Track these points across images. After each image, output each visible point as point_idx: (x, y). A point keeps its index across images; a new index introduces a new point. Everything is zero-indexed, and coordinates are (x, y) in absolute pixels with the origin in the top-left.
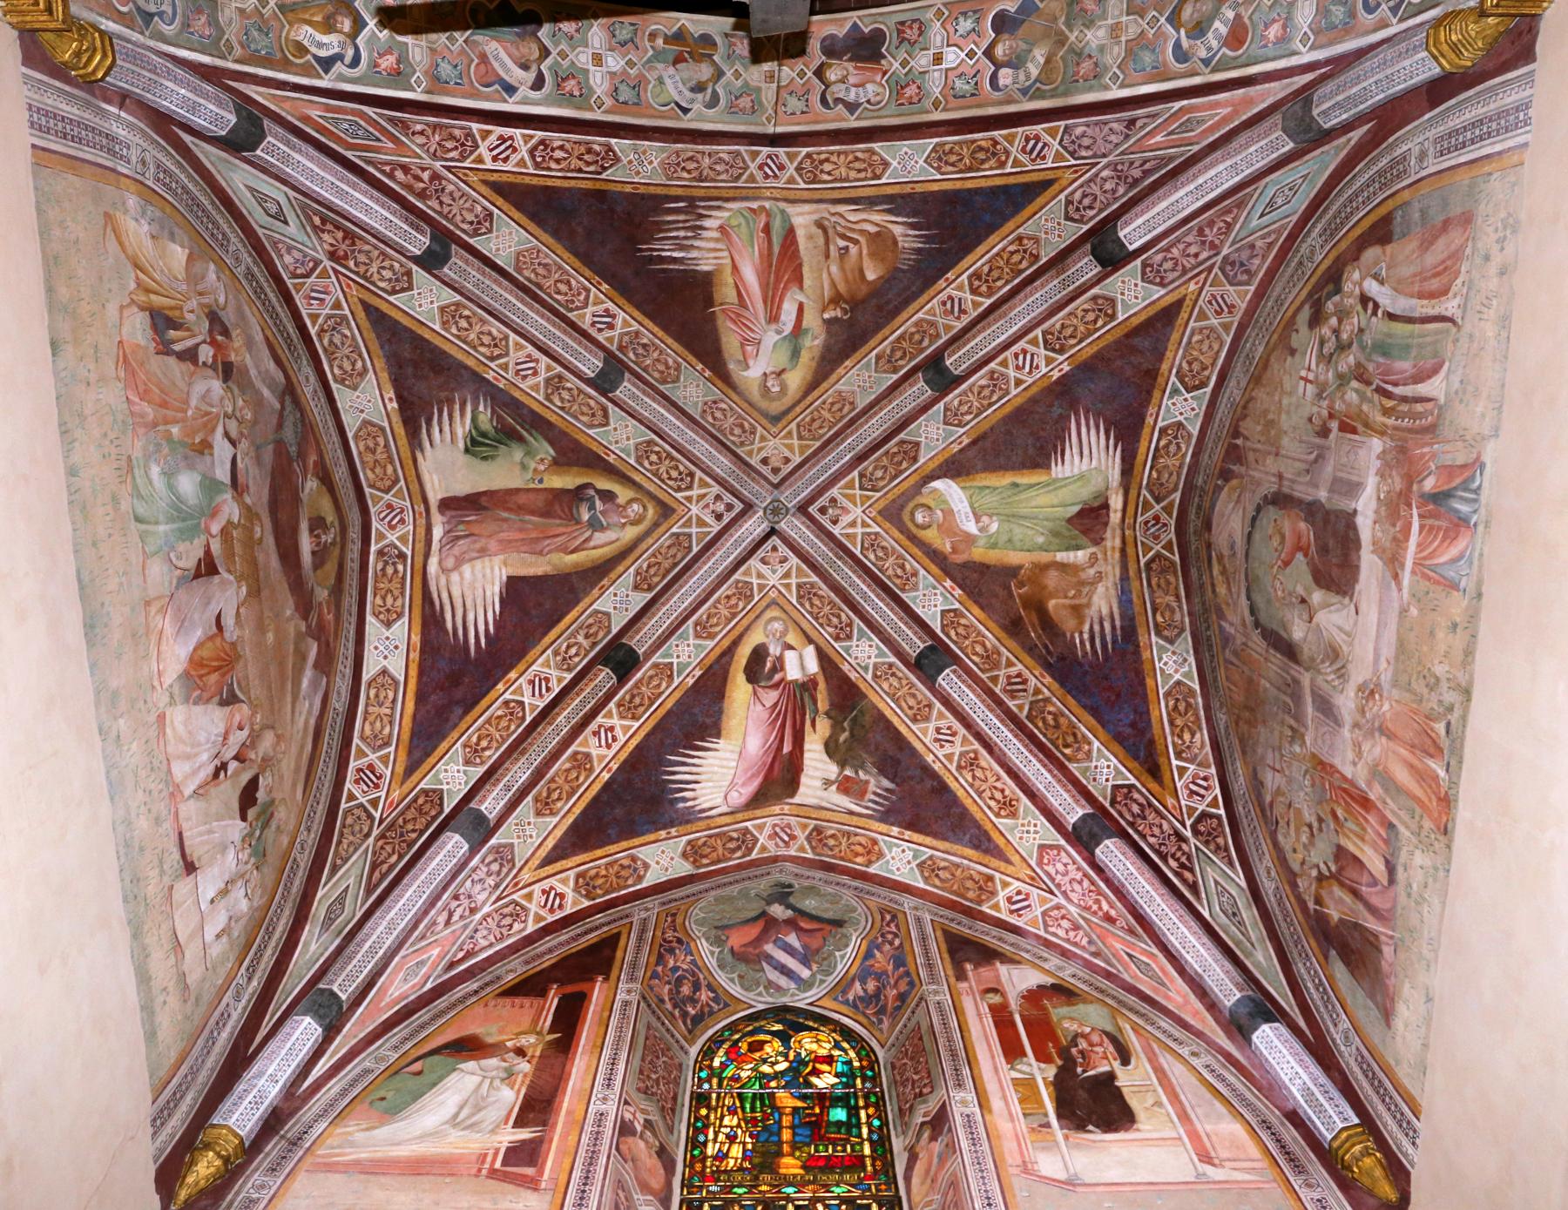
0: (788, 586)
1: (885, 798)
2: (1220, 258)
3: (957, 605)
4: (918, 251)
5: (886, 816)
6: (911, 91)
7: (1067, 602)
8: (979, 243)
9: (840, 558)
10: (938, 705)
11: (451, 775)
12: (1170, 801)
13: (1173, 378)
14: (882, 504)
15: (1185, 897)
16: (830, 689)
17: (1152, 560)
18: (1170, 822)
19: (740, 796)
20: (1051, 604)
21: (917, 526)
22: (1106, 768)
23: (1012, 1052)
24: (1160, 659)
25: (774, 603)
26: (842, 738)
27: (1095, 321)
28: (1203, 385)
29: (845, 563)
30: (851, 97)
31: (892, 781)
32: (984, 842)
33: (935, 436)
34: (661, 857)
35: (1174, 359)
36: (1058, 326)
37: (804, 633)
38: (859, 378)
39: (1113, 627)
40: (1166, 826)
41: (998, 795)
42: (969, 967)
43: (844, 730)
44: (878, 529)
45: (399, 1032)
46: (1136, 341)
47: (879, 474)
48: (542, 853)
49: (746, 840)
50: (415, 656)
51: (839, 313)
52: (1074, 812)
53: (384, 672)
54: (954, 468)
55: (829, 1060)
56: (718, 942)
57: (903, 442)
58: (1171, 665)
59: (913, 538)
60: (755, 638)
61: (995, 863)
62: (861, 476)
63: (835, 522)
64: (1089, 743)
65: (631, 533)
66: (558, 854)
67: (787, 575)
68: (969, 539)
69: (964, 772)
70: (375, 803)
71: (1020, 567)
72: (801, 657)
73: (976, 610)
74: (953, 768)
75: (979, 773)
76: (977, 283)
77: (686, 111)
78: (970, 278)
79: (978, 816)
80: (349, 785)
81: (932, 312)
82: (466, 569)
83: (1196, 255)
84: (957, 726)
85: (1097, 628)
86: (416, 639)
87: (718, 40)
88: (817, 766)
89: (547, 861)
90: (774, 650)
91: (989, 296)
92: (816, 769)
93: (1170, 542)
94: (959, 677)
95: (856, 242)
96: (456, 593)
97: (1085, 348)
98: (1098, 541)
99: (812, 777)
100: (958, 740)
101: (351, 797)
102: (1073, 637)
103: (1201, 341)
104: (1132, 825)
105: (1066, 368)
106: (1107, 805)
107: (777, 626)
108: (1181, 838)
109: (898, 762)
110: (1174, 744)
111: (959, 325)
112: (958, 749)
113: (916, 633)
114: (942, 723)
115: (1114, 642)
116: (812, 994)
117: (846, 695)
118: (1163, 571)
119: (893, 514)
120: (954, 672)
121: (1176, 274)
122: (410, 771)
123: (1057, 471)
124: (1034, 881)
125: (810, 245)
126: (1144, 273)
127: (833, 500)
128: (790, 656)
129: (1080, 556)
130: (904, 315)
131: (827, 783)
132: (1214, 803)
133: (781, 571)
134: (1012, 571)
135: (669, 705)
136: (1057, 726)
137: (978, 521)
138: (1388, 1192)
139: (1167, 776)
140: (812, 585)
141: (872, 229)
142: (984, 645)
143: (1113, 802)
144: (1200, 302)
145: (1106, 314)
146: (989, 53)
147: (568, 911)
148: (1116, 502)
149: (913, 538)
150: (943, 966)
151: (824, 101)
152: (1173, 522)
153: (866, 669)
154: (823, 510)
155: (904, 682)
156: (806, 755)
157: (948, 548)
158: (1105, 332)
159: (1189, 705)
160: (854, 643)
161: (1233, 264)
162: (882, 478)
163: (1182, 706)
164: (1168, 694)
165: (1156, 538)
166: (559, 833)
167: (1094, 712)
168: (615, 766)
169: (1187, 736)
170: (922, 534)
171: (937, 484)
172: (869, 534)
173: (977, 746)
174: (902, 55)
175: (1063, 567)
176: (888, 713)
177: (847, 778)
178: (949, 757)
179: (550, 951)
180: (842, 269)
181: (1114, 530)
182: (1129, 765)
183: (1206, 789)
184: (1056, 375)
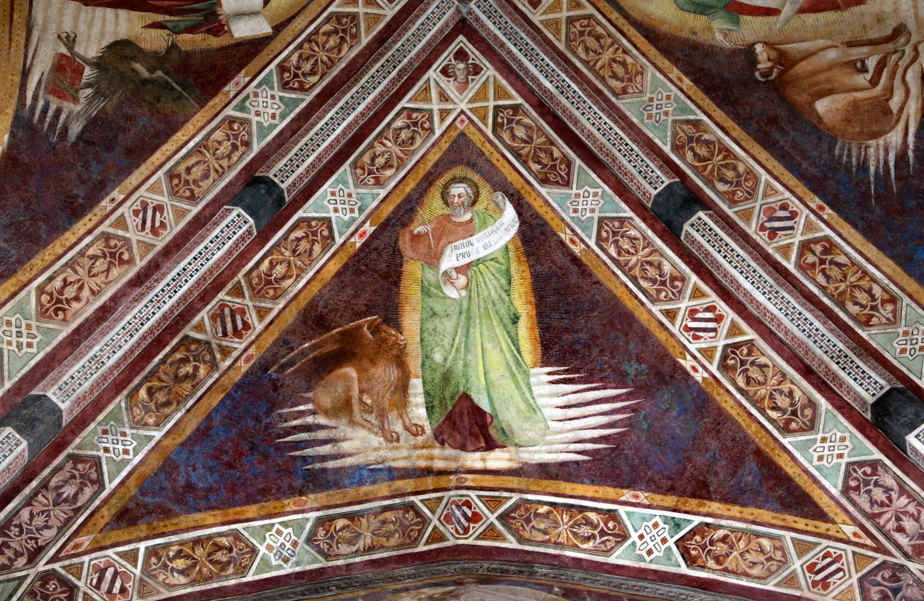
1: (53, 125)
2: (902, 561)
3: (339, 240)
4: (863, 167)
7: (355, 393)
8: (881, 248)
9: (399, 75)
10: (195, 210)
13: (697, 520)
14: (476, 138)
16: (207, 53)
17: (418, 514)
18: (55, 540)
20: (351, 372)
21: (446, 187)
22: (125, 448)
24: (285, 525)
26: (138, 66)
27: (775, 408)
28: (691, 561)
29: (393, 82)
31: (79, 137)
33: (581, 208)
35: (728, 518)
36: (763, 360)
37: (289, 21)
38: (663, 100)
39: (324, 458)
40: (49, 534)
41: (70, 292)
43: (151, 70)
44: (438, 132)
46: (751, 464)
47: (520, 133)
51: (764, 64)
52: (64, 394)
54: (535, 236)
57: (569, 164)
59: (429, 180)
62: (516, 108)
63: (445, 72)
64: (157, 425)
68: (433, 259)
69: (101, 244)
71: (399, 328)
72: (253, 14)
73: (334, 267)
74: (104, 228)
75: (101, 265)
76: (818, 248)
78: (827, 239)
79: (37, 262)
81: (770, 191)
83: (900, 529)
84: (167, 237)
85: (322, 435)
91: (799, 266)
92: (90, 25)
93: (442, 538)
94: (242, 238)
95: (874, 82)
97: (732, 399)
98: (440, 437)
99: (76, 18)
102: (306, 401)
103: (762, 551)
104: (44, 485)
105: (700, 376)
106: (69, 450)
108: (34, 556)
109: (109, 148)
110: (167, 546)
111: (751, 229)
112: (133, 236)
113: (300, 178)
114: (169, 215)
115: (304, 459)
118: (404, 529)
119: (461, 153)
120: (249, 232)
121: (866, 507)
123: (540, 376)
125: (867, 20)
126: (861, 464)
127: (477, 70)
129: (418, 412)
130: (763, 155)
131: (70, 41)
134: (392, 317)
136: (177, 379)
137: (458, 270)
139: (123, 535)
140: (356, 37)
141: (895, 103)
142: (284, 277)
143: (75, 459)
144: (825, 543)
145: (788, 422)
148: (497, 460)
149: (429, 180)
152: (470, 541)
153: (242, 108)
154: (461, 55)
155: (225, 163)
156: (110, 12)
157: (418, 229)
158: (761, 424)
159: (224, 566)
160: (278, 93)
161: (894, 578)
162: (514, 137)
163: (221, 556)
164: (237, 536)
167: (203, 432)
169: (180, 564)
171: (510, 213)
172: (430, 119)
173: (140, 264)
175: (403, 387)
176: (179, 137)
177: (79, 71)
178: (121, 223)
180: (832, 66)
181: (456, 459)
182: (132, 482)
183: (109, 591)
184: (687, 363)
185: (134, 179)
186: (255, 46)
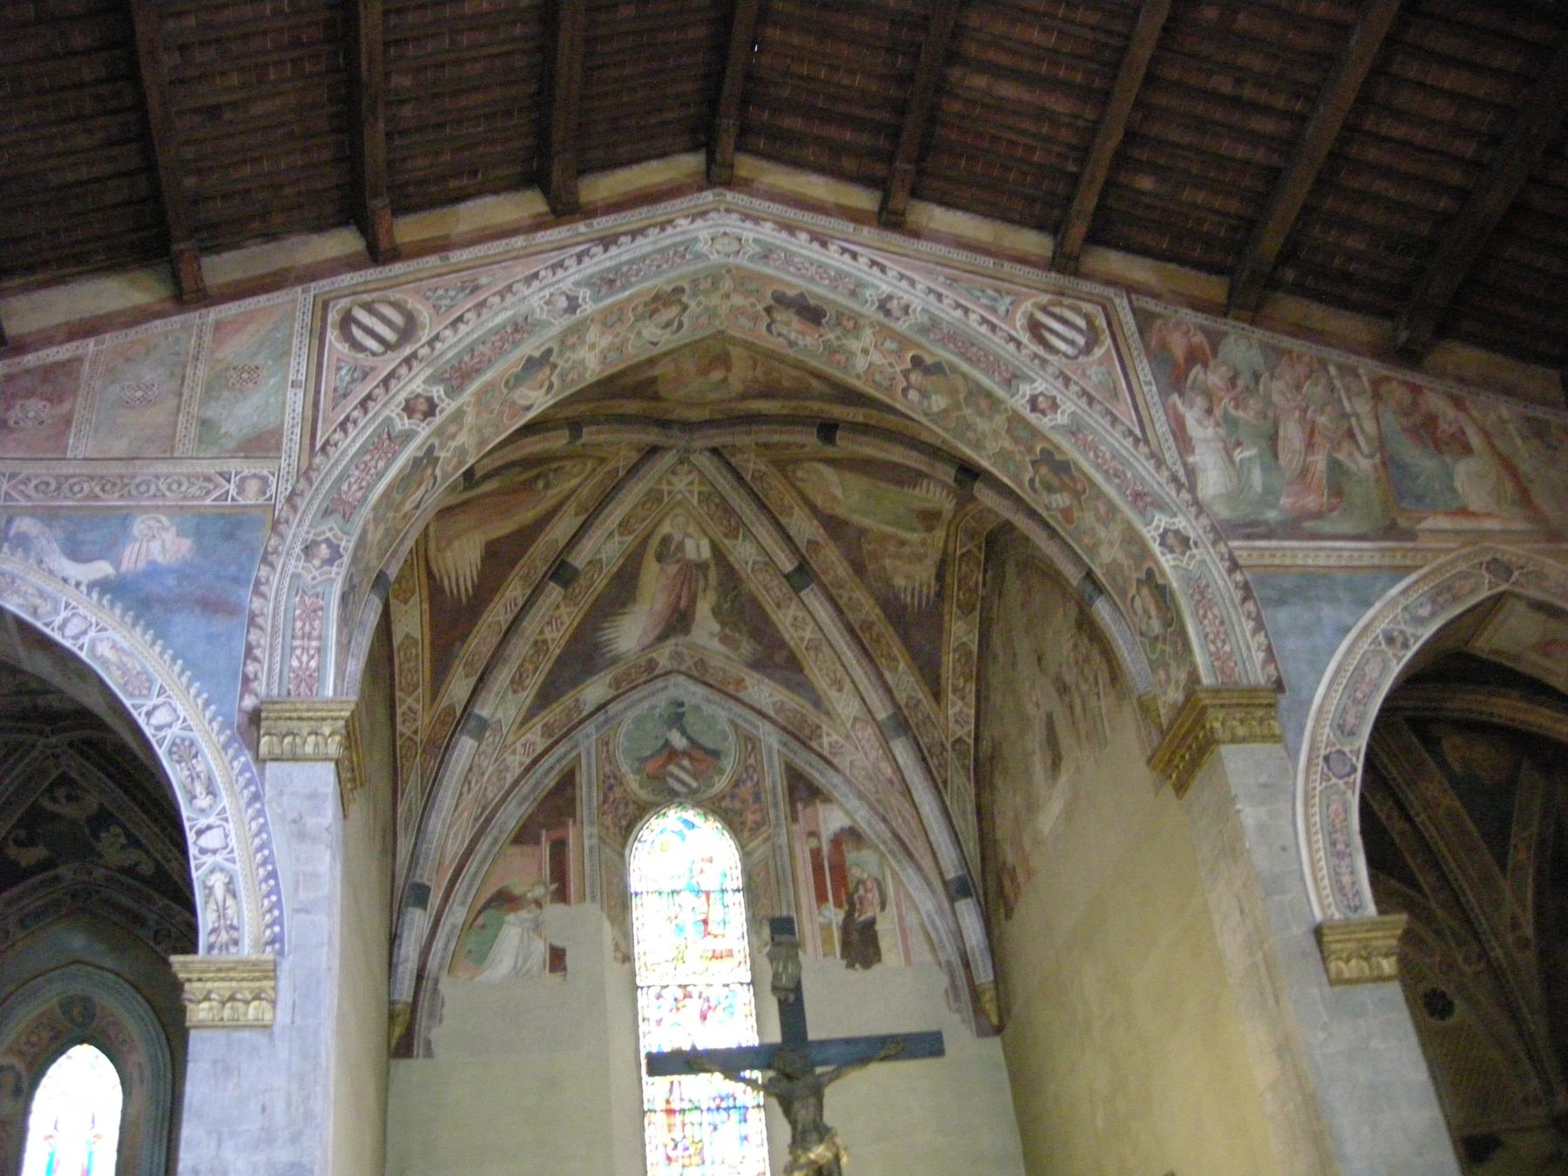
0: (691, 492)
5: (755, 665)
6: (841, 357)
11: (458, 688)
12: (942, 720)
15: (939, 788)
19: (647, 641)
22: (905, 680)
23: (821, 897)
30: (793, 336)
32: (817, 702)
34: (594, 691)
42: (800, 806)
45: (461, 887)
48: (519, 720)
49: (651, 665)
50: (427, 617)
53: (407, 636)
56: (638, 771)
58: (960, 631)
59: (794, 487)
60: (666, 528)
61: (823, 717)
65: (574, 482)
66: (532, 713)
67: (691, 483)
68: (834, 498)
70: (416, 732)
77: (655, 344)
80: (399, 727)
82: (456, 544)
84: (808, 618)
86: (426, 606)
87: (686, 286)
89: (523, 723)
90: (677, 537)
96: (451, 567)
98: (930, 529)
101: (402, 735)
117: (730, 576)
122: (434, 697)
124: (848, 737)
129: (915, 537)
133: (686, 480)
135: (600, 588)
136: (878, 641)
146: (906, 373)
147: (538, 751)
150: (783, 806)
151: (769, 327)
164: (955, 650)
166: (529, 701)
168: (563, 642)
170: (798, 484)
171: (821, 467)
174: (838, 332)
185: (780, 626)
186: (715, 547)
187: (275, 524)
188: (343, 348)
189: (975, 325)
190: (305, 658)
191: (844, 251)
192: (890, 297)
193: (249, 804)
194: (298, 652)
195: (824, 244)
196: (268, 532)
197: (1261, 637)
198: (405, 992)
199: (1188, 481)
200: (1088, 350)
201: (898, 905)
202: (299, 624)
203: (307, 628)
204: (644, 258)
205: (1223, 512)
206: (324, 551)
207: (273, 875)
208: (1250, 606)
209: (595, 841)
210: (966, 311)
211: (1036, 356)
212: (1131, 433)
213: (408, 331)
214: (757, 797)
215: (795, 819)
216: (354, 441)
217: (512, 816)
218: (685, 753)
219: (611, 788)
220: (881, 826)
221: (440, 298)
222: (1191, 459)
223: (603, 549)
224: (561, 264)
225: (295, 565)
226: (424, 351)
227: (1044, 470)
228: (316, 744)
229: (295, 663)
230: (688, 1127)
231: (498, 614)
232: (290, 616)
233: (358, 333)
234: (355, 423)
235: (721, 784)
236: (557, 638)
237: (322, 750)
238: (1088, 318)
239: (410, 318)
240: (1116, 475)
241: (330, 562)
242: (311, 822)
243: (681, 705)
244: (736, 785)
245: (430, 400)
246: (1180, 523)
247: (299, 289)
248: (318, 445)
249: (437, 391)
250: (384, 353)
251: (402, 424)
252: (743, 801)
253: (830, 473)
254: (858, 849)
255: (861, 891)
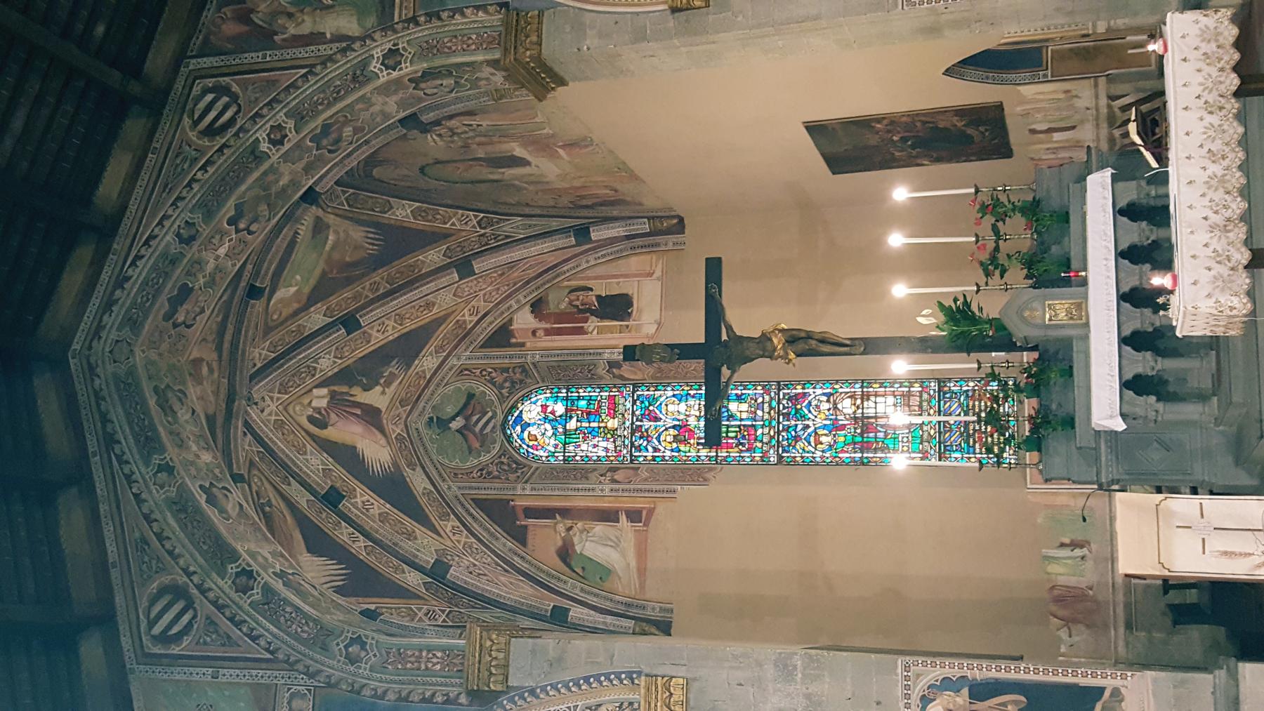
5: (409, 366)
11: (413, 579)
19: (383, 441)
20: (348, 259)
22: (433, 257)
25: (285, 409)
32: (439, 322)
34: (418, 482)
42: (513, 340)
45: (553, 583)
49: (399, 438)
55: (544, 407)
58: (403, 212)
59: (282, 323)
67: (272, 398)
77: (194, 411)
88: (376, 397)
90: (310, 412)
98: (328, 227)
100: (387, 322)
101: (444, 621)
107: (297, 408)
112: (392, 323)
116: (499, 411)
117: (345, 376)
124: (468, 302)
128: (314, 404)
131: (383, 393)
132: (476, 217)
134: (324, 274)
136: (402, 273)
138: (675, 221)
146: (237, 231)
149: (282, 323)
165: (337, 197)
174: (201, 276)
175: (333, 248)
178: (394, 328)
179: (487, 530)
186: (320, 385)
187: (329, 685)
188: (186, 641)
189: (207, 176)
190: (435, 660)
191: (133, 264)
192: (178, 235)
193: (538, 697)
194: (430, 665)
195: (128, 279)
196: (335, 691)
197: (468, 12)
198: (629, 624)
199: (346, 42)
200: (234, 98)
201: (589, 279)
202: (409, 665)
203: (412, 659)
204: (128, 415)
205: (371, 21)
206: (354, 649)
207: (586, 680)
208: (444, 15)
209: (528, 486)
210: (193, 180)
211: (236, 135)
212: (304, 75)
213: (178, 592)
214: (506, 370)
215: (523, 345)
216: (267, 630)
217: (505, 544)
218: (467, 419)
219: (489, 473)
220: (532, 285)
221: (150, 568)
222: (328, 36)
223: (314, 464)
224: (128, 477)
225: (364, 670)
226: (196, 579)
227: (325, 142)
228: (498, 650)
229: (438, 667)
230: (731, 435)
231: (359, 546)
232: (402, 672)
233: (175, 630)
234: (252, 630)
235: (491, 394)
236: (378, 506)
237: (503, 646)
238: (206, 91)
239: (162, 591)
240: (338, 93)
241: (363, 645)
242: (552, 654)
243: (431, 419)
244: (494, 384)
245: (238, 575)
246: (377, 53)
247: (131, 677)
248: (269, 656)
249: (232, 569)
250: (195, 610)
251: (257, 594)
252: (505, 381)
253: (279, 294)
254: (547, 303)
255: (578, 303)
